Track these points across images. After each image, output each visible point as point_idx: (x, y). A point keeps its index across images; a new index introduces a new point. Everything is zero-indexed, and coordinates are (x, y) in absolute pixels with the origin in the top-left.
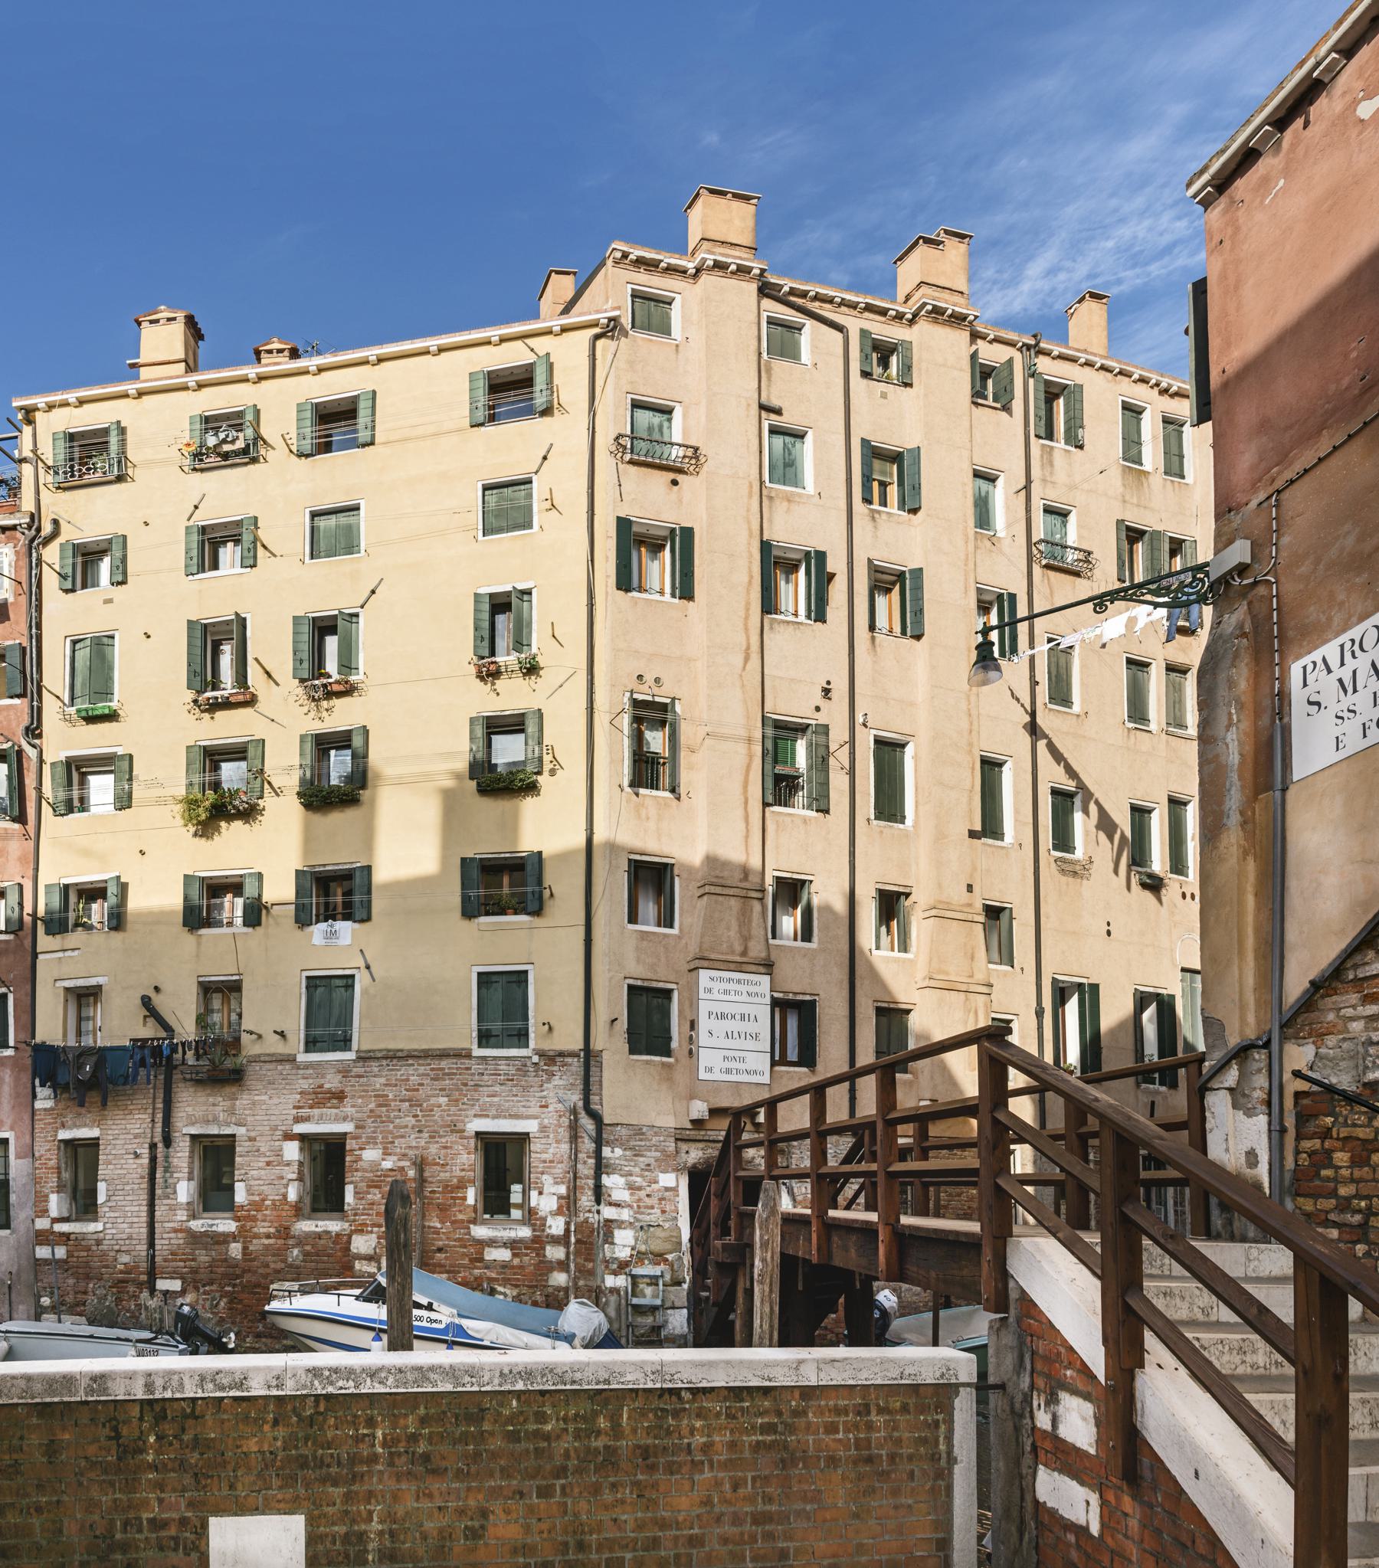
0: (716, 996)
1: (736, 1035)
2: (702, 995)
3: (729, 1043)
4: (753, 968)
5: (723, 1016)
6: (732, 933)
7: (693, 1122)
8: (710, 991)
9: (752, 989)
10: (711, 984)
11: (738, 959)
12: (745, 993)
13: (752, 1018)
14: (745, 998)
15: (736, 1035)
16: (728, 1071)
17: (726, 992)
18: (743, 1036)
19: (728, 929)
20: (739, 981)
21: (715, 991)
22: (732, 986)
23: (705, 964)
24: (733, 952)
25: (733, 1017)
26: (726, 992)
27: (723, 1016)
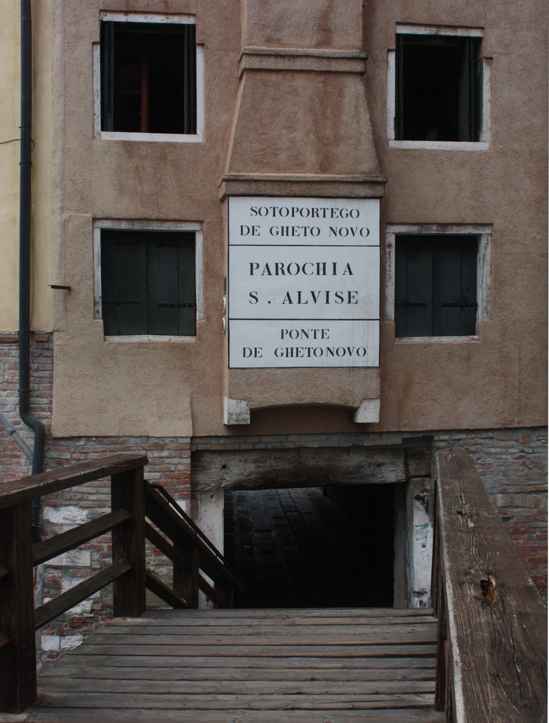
0: (264, 237)
1: (306, 296)
2: (235, 236)
3: (295, 310)
4: (343, 190)
5: (280, 269)
6: (298, 135)
7: (229, 427)
8: (253, 231)
9: (338, 223)
10: (251, 221)
11: (310, 176)
12: (325, 231)
13: (341, 268)
14: (326, 237)
15: (306, 296)
16: (290, 352)
17: (285, 231)
18: (322, 298)
19: (291, 127)
20: (313, 213)
21: (264, 230)
22: (298, 221)
23: (241, 188)
24: (300, 166)
25: (301, 269)
26: (285, 231)
27: (280, 269)
